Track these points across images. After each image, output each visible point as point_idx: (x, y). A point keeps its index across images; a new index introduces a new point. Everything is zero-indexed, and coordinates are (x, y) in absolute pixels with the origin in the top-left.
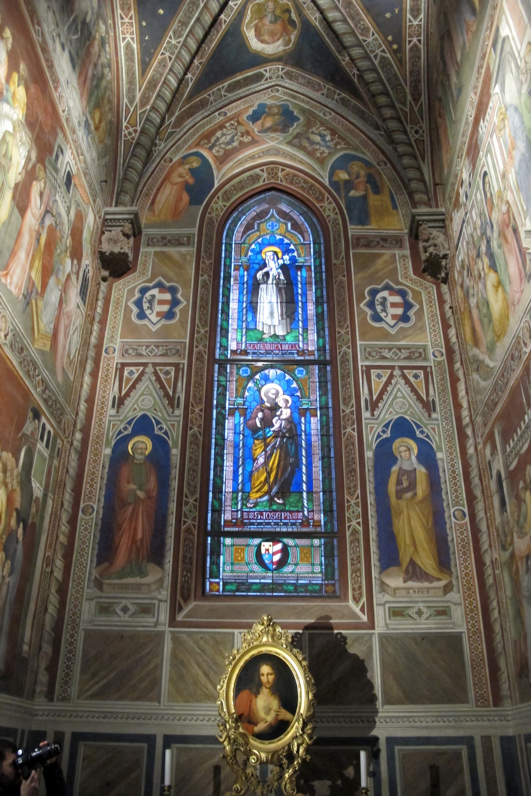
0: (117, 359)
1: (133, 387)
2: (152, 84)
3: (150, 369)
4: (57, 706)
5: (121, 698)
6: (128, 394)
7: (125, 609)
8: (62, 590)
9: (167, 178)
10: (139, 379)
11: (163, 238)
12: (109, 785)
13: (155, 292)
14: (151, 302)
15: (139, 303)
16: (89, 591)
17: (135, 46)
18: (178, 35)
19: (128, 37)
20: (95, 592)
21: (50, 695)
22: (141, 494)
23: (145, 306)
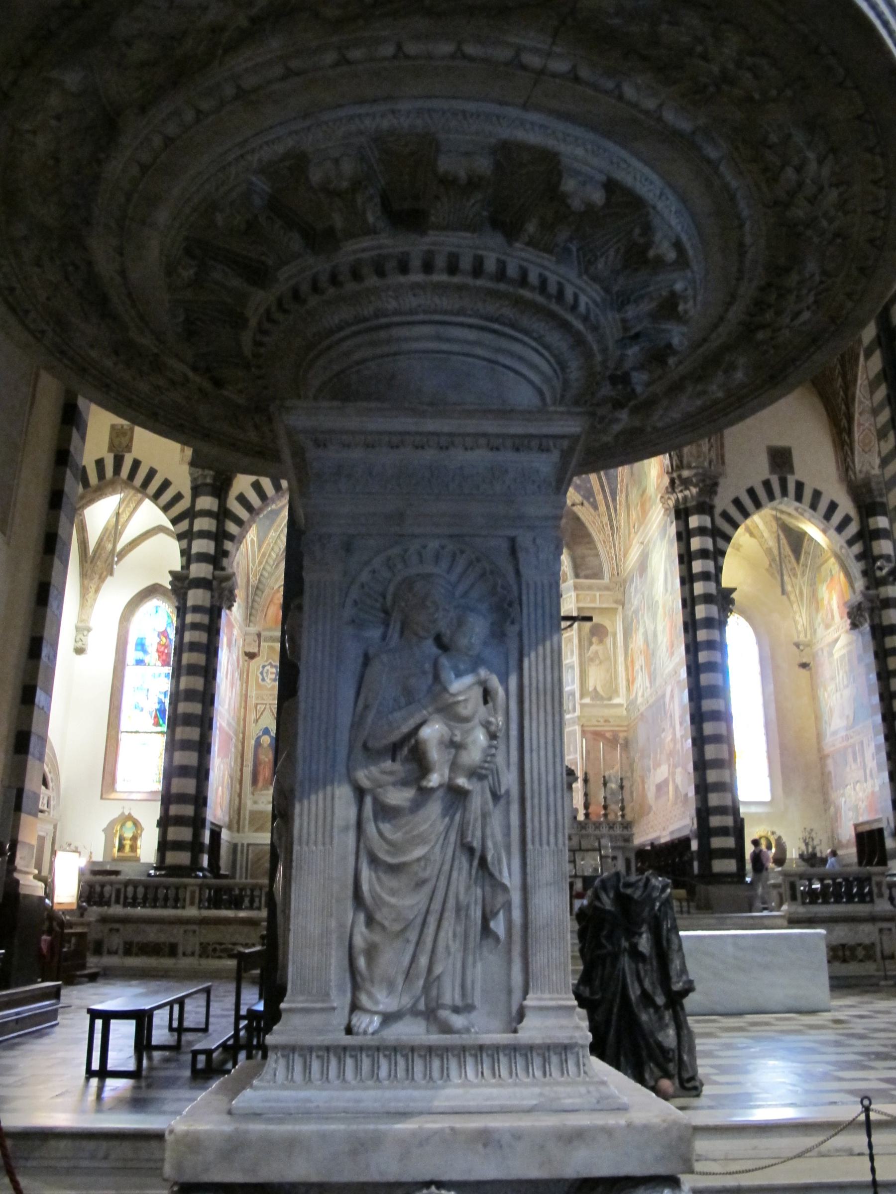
0: (254, 701)
1: (262, 714)
2: (264, 555)
3: (268, 706)
4: (241, 835)
5: (263, 832)
6: (259, 718)
7: (263, 802)
8: (240, 796)
9: (271, 601)
10: (264, 710)
11: (271, 637)
12: (259, 859)
13: (268, 667)
14: (267, 673)
15: (262, 673)
16: (249, 796)
17: (255, 539)
18: (275, 531)
19: (252, 536)
20: (251, 796)
21: (238, 831)
22: (267, 760)
23: (265, 675)
